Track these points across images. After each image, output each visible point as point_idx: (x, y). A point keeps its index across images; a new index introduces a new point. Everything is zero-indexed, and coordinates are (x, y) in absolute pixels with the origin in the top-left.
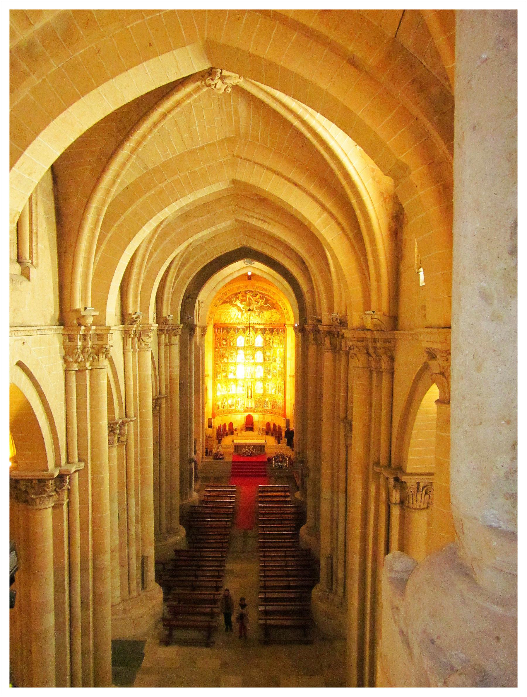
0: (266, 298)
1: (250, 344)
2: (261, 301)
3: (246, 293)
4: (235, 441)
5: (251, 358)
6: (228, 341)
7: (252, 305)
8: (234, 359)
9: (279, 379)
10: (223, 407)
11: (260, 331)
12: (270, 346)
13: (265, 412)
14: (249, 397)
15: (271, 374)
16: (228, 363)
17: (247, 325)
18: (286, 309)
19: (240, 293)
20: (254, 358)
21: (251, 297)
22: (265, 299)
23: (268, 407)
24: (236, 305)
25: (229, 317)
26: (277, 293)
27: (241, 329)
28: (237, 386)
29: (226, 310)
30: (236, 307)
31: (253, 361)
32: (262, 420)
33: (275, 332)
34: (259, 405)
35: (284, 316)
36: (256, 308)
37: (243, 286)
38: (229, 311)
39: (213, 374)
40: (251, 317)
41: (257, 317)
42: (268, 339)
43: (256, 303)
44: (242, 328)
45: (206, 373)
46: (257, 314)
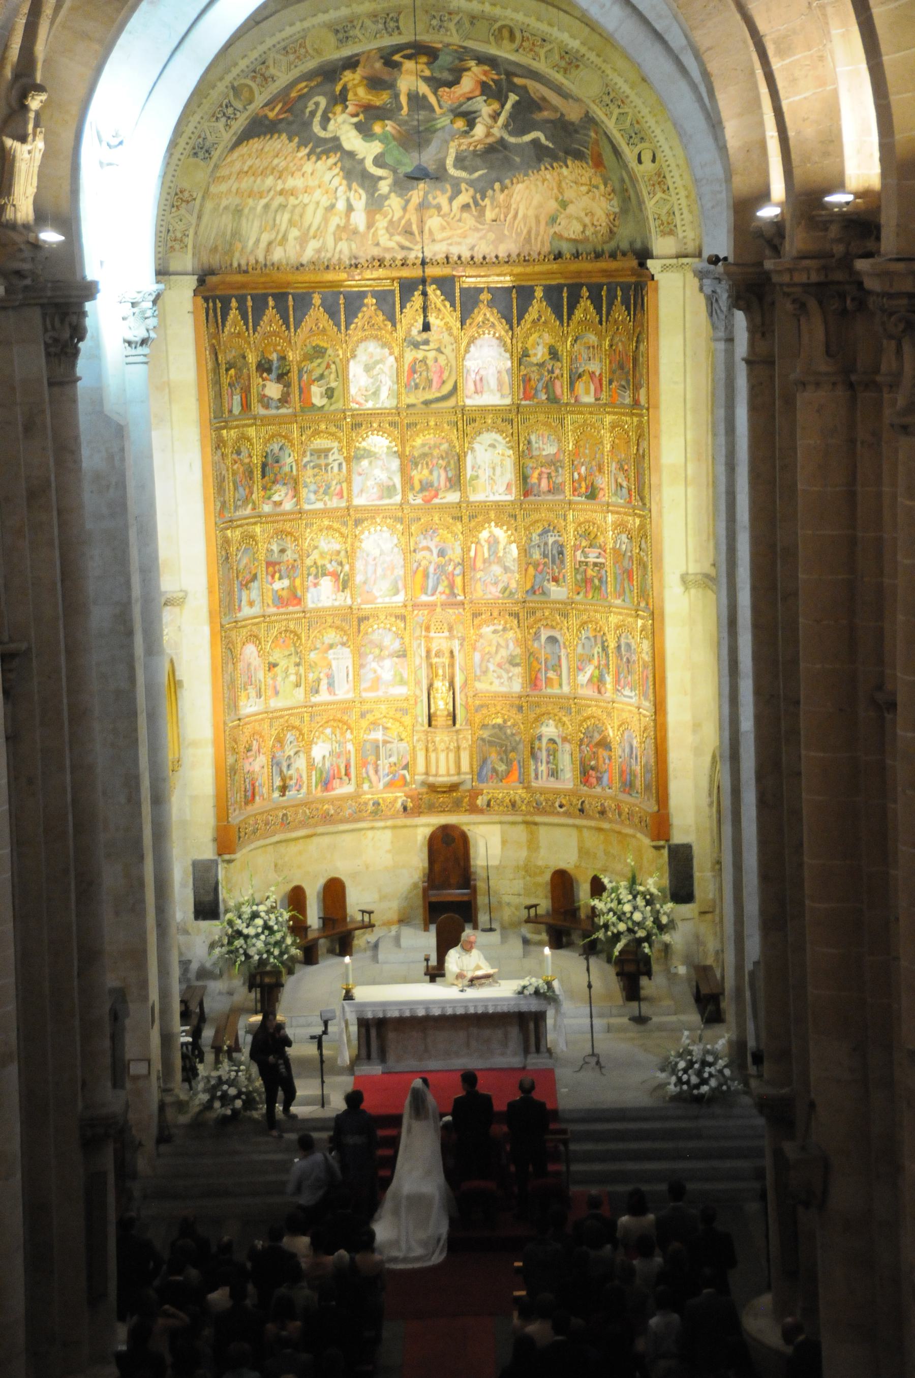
0: (522, 91)
1: (429, 396)
2: (485, 109)
3: (397, 66)
4: (365, 994)
5: (440, 478)
6: (294, 376)
8: (335, 488)
9: (618, 602)
10: (284, 789)
11: (491, 304)
12: (553, 400)
13: (539, 809)
14: (441, 720)
17: (405, 273)
18: (647, 157)
19: (351, 63)
20: (456, 481)
21: (424, 89)
22: (513, 98)
23: (554, 773)
24: (334, 146)
25: (291, 223)
26: (592, 56)
27: (370, 301)
28: (359, 655)
29: (270, 181)
30: (332, 161)
31: (453, 497)
32: (524, 853)
33: (585, 305)
34: (502, 768)
35: (640, 203)
36: (460, 162)
37: (374, 16)
38: (291, 183)
40: (434, 222)
41: (469, 219)
42: (539, 354)
43: (460, 124)
44: (376, 294)
45: (168, 584)
46: (465, 197)
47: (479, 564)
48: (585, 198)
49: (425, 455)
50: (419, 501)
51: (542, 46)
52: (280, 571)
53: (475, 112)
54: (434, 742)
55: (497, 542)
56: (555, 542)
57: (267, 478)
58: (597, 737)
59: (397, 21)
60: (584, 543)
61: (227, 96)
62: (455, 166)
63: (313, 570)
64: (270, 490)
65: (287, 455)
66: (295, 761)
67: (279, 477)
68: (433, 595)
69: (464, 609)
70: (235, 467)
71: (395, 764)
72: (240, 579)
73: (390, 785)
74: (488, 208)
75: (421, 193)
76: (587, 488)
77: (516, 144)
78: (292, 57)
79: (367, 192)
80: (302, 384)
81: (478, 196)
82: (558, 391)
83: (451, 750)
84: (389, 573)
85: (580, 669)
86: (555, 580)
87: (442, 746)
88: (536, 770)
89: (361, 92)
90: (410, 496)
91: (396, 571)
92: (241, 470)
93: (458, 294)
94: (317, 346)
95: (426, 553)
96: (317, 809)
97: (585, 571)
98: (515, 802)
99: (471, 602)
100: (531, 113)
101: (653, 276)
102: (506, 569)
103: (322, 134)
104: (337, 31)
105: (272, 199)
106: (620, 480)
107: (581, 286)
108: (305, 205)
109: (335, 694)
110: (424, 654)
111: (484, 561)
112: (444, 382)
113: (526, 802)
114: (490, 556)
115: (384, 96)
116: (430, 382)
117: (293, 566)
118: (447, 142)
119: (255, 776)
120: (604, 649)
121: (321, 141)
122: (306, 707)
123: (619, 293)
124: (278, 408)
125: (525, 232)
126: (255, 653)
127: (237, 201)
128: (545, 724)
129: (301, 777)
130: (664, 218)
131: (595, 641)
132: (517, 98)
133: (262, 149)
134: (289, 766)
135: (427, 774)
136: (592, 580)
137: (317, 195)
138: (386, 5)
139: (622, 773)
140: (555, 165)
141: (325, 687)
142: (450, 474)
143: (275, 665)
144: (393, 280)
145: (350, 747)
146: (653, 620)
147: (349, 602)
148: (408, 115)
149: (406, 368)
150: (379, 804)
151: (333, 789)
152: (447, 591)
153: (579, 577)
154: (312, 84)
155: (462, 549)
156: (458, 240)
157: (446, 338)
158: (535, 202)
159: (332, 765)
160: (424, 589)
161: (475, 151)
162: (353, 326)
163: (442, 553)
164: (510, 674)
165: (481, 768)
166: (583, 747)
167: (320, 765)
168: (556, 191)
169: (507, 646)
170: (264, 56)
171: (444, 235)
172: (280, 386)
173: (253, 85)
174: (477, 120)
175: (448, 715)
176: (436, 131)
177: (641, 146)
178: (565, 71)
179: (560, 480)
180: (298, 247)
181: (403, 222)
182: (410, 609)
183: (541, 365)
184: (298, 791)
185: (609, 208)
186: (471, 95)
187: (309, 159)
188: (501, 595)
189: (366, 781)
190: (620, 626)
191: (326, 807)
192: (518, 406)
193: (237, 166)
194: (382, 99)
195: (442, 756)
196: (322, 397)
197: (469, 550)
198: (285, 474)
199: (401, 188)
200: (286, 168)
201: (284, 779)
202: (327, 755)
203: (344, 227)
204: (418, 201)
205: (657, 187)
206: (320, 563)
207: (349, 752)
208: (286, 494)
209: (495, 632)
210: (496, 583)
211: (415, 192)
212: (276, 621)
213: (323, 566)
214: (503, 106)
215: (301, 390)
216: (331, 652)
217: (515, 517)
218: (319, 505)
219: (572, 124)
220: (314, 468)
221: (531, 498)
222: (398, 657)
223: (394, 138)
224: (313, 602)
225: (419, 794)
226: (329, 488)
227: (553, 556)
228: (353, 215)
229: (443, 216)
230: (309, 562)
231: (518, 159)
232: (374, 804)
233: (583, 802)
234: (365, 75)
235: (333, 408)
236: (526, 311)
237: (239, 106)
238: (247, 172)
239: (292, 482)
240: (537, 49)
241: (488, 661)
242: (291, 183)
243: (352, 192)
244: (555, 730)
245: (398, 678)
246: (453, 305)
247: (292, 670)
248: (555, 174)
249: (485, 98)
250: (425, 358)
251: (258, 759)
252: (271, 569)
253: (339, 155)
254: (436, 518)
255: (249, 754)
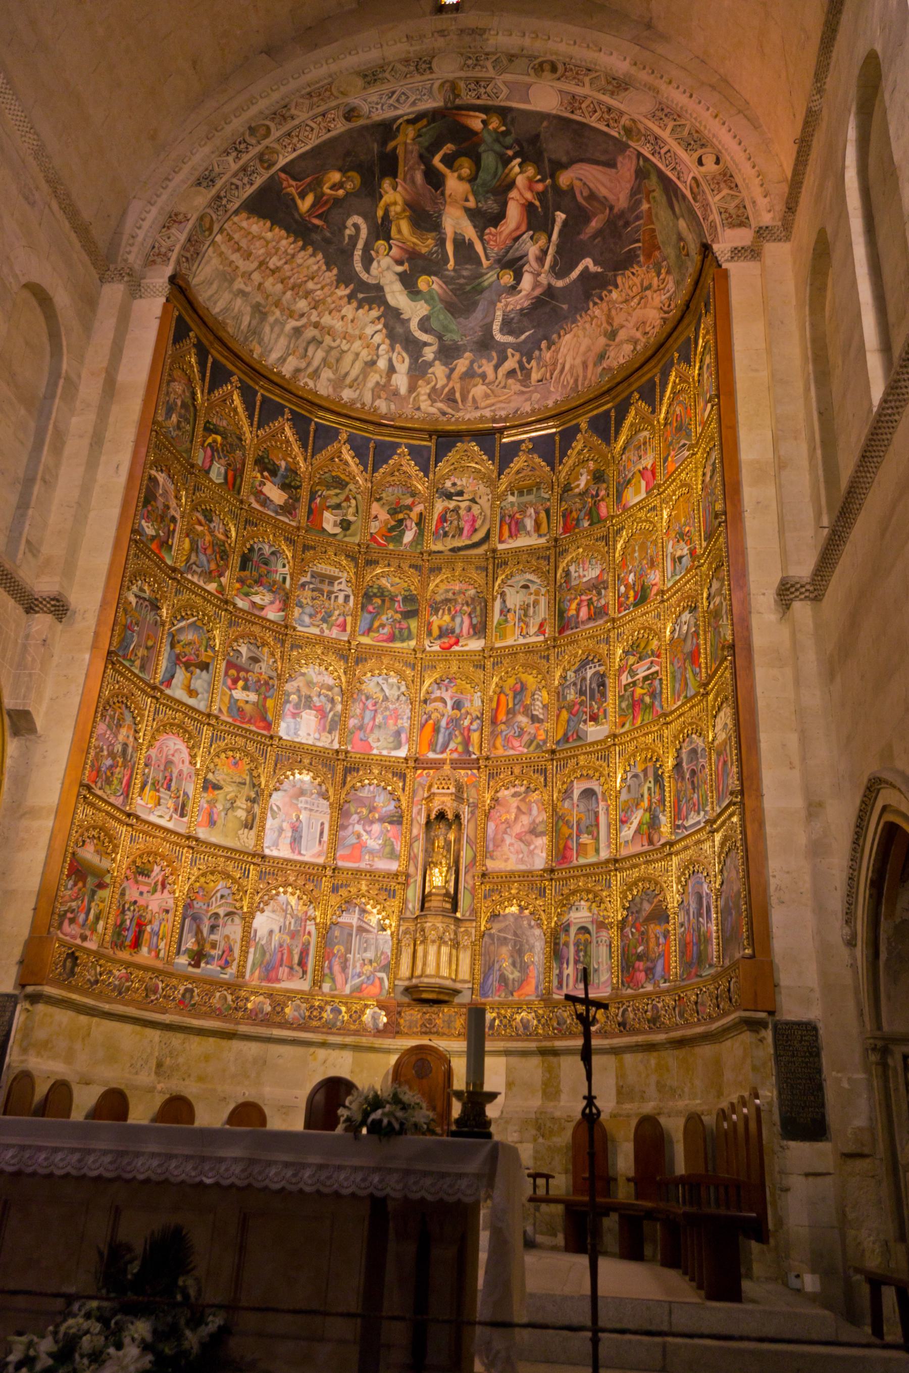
5: (463, 624)
6: (304, 494)
7: (480, 307)
10: (198, 957)
11: (530, 451)
15: (611, 702)
16: (286, 627)
18: (709, 160)
21: (469, 232)
22: (560, 216)
25: (324, 360)
26: (643, 76)
29: (302, 305)
30: (375, 313)
31: (476, 645)
32: (536, 1102)
34: (517, 974)
36: (508, 326)
37: (407, 61)
39: (104, 603)
40: (478, 390)
42: (583, 481)
43: (508, 278)
44: (407, 446)
46: (511, 363)
47: (502, 717)
48: (634, 314)
49: (447, 601)
50: (436, 648)
51: (586, 75)
52: (246, 680)
53: (521, 258)
54: (423, 930)
55: (523, 687)
56: (595, 674)
57: (247, 573)
58: (647, 907)
59: (430, 63)
60: (632, 659)
61: (243, 134)
62: (501, 331)
63: (294, 698)
64: (250, 586)
65: (280, 565)
66: (225, 925)
67: (265, 580)
68: (442, 752)
69: (479, 769)
70: (199, 528)
71: (371, 962)
72: (177, 650)
73: (359, 989)
74: (534, 370)
75: (467, 362)
76: (635, 598)
77: (564, 288)
78: (315, 99)
79: (411, 357)
80: (313, 506)
81: (524, 360)
82: (603, 511)
83: (445, 943)
84: (391, 722)
85: (623, 822)
86: (594, 718)
87: (433, 935)
88: (560, 976)
89: (405, 226)
90: (427, 642)
91: (400, 722)
92: (208, 538)
93: (497, 449)
94: (338, 477)
95: (439, 705)
96: (247, 1000)
97: (633, 692)
98: (528, 1021)
99: (487, 758)
100: (579, 233)
101: (720, 266)
102: (534, 719)
103: (364, 276)
104: (366, 76)
105: (304, 326)
106: (679, 553)
107: (630, 396)
108: (344, 352)
109: (300, 853)
110: (423, 821)
111: (508, 713)
112: (475, 530)
113: (543, 1021)
114: (515, 705)
115: (430, 241)
116: (461, 530)
117: (266, 683)
118: (493, 304)
119: (149, 917)
120: (658, 779)
121: (362, 286)
122: (254, 856)
123: (676, 355)
124: (277, 513)
125: (572, 382)
126: (187, 759)
127: (259, 298)
128: (574, 908)
129: (231, 950)
130: (732, 211)
131: (646, 775)
132: (563, 216)
133: (293, 256)
134: (213, 928)
135: (410, 978)
136: (641, 700)
137: (357, 345)
138: (418, 48)
139: (684, 947)
140: (605, 292)
141: (288, 841)
142: (475, 621)
143: (216, 787)
144: (431, 433)
145: (311, 927)
146: (734, 655)
147: (336, 746)
148: (454, 270)
149: (436, 517)
150: (340, 1012)
151: (278, 980)
152: (460, 749)
153: (624, 705)
154: (349, 186)
155: (483, 702)
156: (503, 405)
157: (482, 489)
158: (583, 348)
159: (281, 946)
160: (432, 746)
161: (522, 310)
162: (381, 470)
163: (457, 705)
164: (532, 847)
165: (486, 976)
166: (627, 929)
167: (263, 942)
168: (605, 325)
169: (530, 810)
170: (287, 100)
171: (488, 402)
172: (285, 496)
173: (272, 125)
174: (526, 268)
175: (447, 894)
176: (482, 291)
177: (700, 152)
178: (612, 93)
179: (603, 602)
180: (331, 390)
181: (447, 390)
182: (411, 764)
183: (583, 494)
184: (223, 968)
185: (663, 297)
186: (518, 233)
187: (349, 303)
188: (525, 750)
189: (327, 979)
190: (681, 731)
191: (261, 998)
192: (556, 540)
193: (259, 251)
194: (426, 245)
195: (432, 950)
196: (335, 525)
197: (491, 700)
198: (275, 582)
199: (447, 357)
200: (323, 301)
201: (200, 941)
202: (276, 929)
203: (384, 386)
204: (464, 369)
205: (722, 185)
206: (304, 691)
207: (309, 933)
208: (272, 603)
209: (515, 795)
210: (520, 735)
211: (461, 361)
212: (229, 733)
213: (309, 698)
214: (550, 237)
215: (310, 511)
216: (302, 799)
217: (547, 658)
218: (316, 631)
219: (622, 214)
220: (313, 590)
221: (569, 632)
222: (391, 823)
223: (441, 300)
224: (288, 735)
225: (400, 1005)
226: (330, 616)
227: (592, 690)
228: (394, 376)
229: (488, 385)
230: (289, 687)
231: (565, 307)
232: (332, 1010)
233: (625, 1011)
234: (407, 197)
235: (346, 539)
236: (570, 447)
237: (254, 142)
238: (273, 272)
239: (282, 593)
240: (581, 77)
241: (505, 832)
242: (326, 320)
243: (395, 354)
244: (590, 915)
245: (388, 849)
246: (492, 458)
247: (242, 803)
248: (604, 305)
249: (531, 233)
250: (459, 507)
251: (158, 895)
252: (233, 672)
253: (382, 309)
254: (454, 669)
255: (140, 878)
